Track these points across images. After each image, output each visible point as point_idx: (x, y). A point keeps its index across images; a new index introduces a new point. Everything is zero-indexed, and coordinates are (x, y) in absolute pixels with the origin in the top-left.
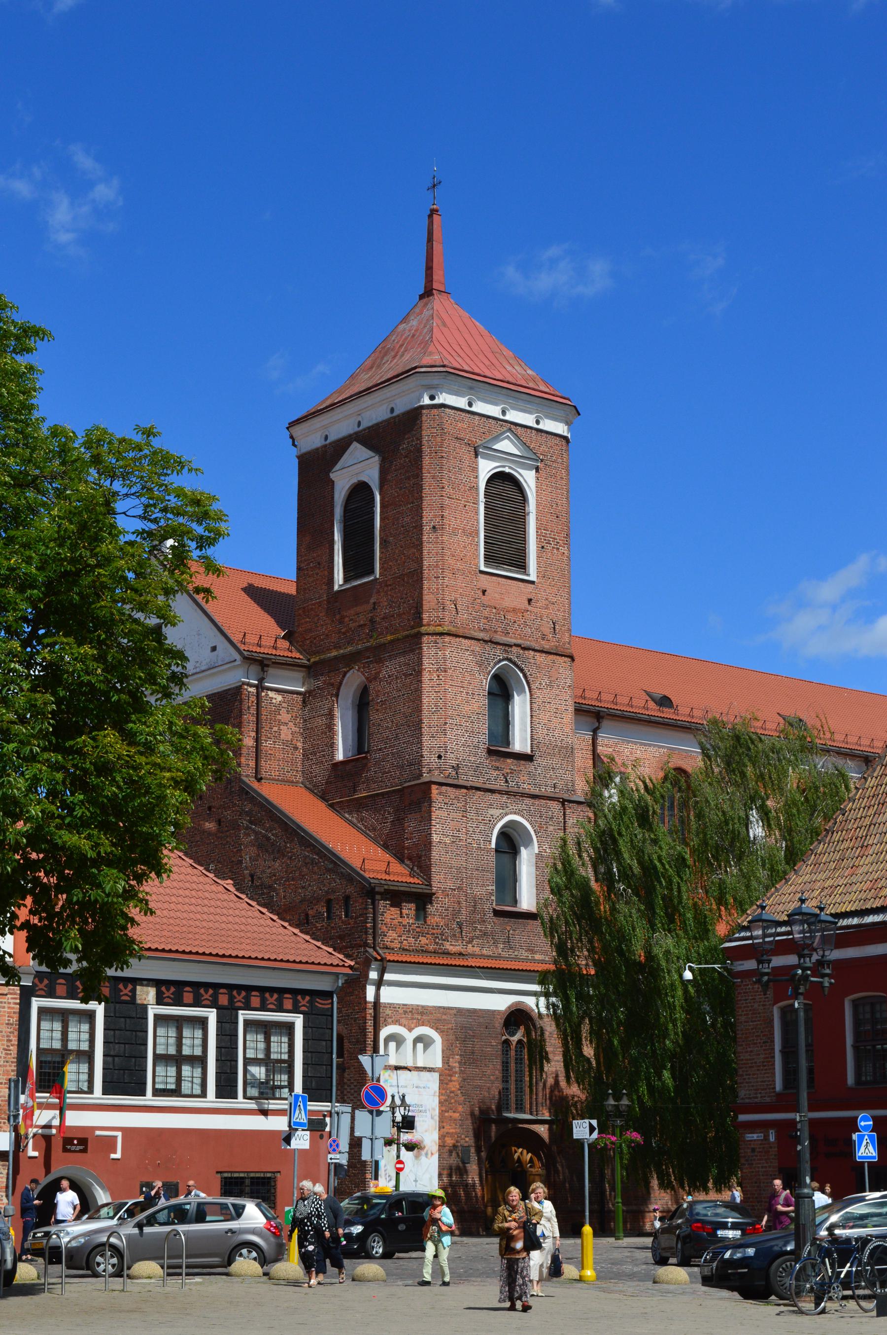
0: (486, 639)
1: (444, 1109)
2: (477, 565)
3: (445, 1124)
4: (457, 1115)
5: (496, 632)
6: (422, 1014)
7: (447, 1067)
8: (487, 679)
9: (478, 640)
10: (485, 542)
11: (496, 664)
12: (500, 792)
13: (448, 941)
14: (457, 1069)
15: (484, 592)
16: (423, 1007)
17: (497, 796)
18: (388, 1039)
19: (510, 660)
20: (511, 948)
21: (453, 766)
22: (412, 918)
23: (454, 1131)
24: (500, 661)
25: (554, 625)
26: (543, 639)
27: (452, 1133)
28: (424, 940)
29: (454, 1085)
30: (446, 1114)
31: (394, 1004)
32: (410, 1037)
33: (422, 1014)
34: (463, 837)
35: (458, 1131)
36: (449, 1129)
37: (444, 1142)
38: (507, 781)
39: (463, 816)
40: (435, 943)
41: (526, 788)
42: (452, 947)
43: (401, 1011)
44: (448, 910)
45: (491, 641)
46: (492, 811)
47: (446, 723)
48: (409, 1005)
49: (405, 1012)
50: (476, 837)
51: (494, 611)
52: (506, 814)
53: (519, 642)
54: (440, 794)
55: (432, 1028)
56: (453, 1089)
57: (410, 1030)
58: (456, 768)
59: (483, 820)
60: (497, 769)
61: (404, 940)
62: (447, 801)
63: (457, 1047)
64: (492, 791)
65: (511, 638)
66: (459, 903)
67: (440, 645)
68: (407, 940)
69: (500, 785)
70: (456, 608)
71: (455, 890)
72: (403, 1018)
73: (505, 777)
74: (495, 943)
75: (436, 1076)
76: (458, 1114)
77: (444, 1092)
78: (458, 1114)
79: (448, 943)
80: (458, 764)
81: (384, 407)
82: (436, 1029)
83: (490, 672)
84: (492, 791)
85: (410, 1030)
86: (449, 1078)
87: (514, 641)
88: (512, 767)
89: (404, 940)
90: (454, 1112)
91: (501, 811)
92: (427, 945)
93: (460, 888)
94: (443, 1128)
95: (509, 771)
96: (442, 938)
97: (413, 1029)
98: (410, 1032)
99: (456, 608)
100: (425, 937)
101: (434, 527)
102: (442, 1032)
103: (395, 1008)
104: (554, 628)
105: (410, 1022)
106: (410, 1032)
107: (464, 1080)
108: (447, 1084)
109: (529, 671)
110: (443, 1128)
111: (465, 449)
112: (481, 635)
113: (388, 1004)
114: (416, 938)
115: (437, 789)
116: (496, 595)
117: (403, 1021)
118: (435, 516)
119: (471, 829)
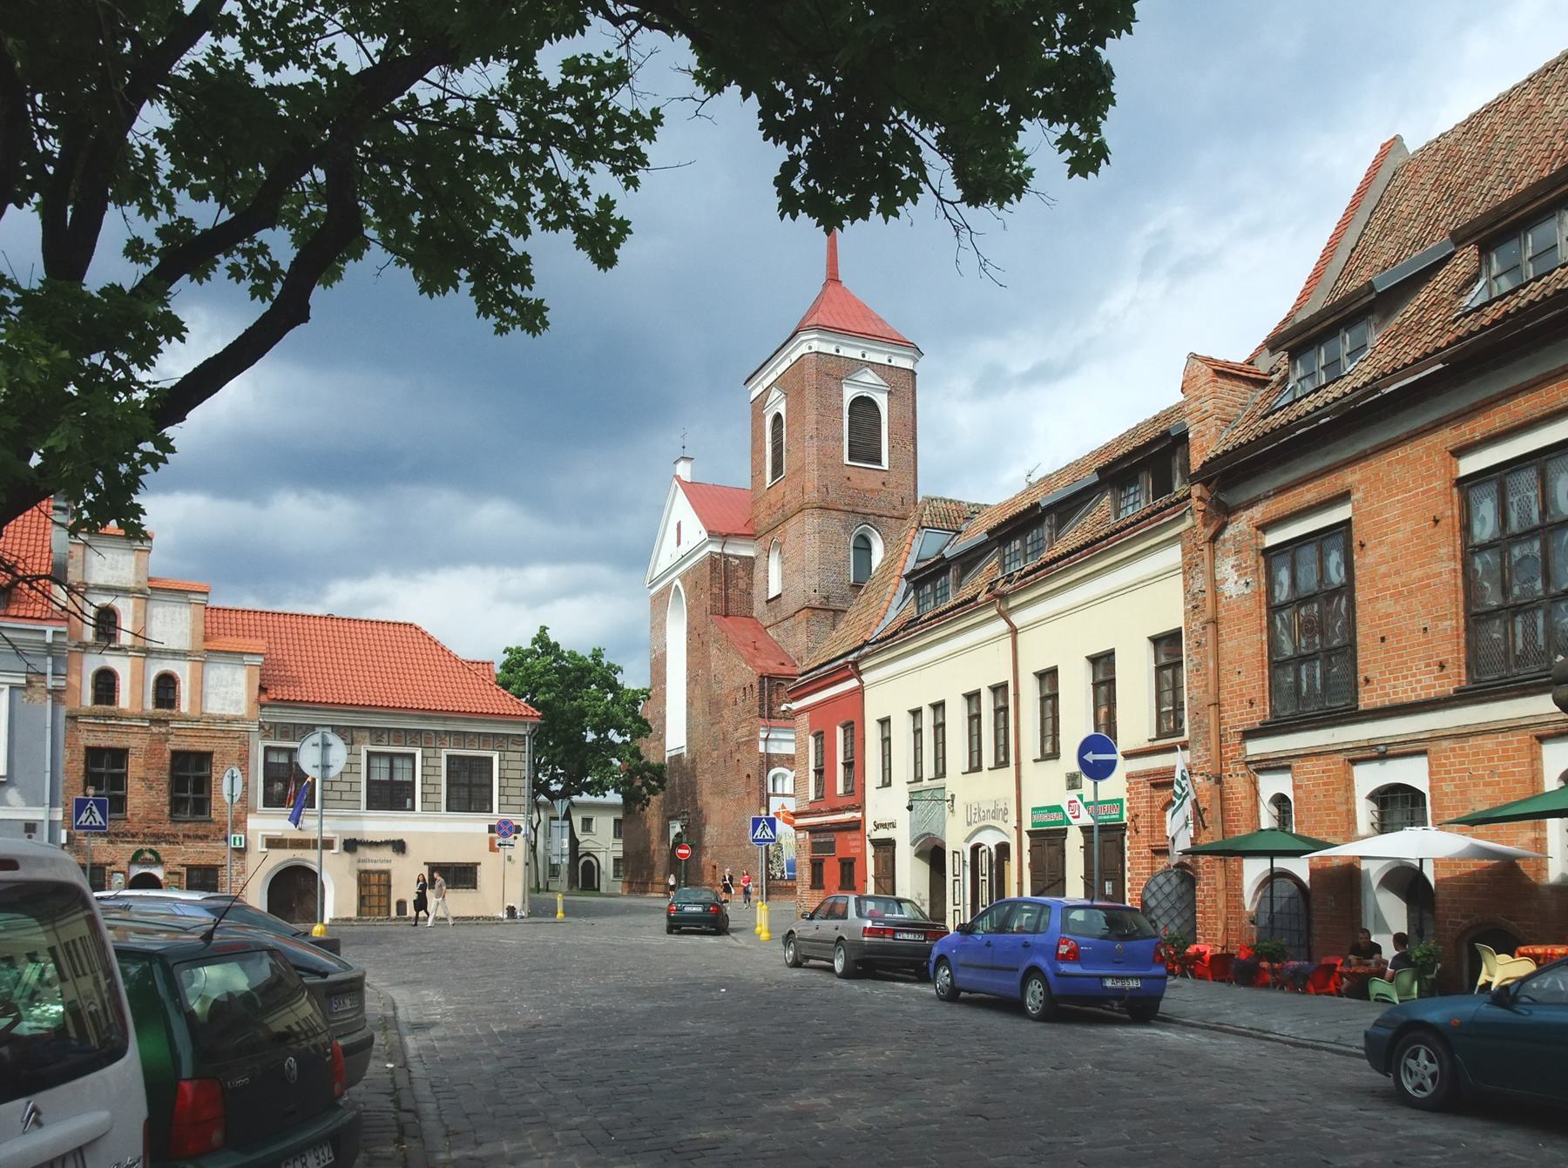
58: (827, 598)
87: (871, 511)
112: (846, 508)
117: (786, 765)
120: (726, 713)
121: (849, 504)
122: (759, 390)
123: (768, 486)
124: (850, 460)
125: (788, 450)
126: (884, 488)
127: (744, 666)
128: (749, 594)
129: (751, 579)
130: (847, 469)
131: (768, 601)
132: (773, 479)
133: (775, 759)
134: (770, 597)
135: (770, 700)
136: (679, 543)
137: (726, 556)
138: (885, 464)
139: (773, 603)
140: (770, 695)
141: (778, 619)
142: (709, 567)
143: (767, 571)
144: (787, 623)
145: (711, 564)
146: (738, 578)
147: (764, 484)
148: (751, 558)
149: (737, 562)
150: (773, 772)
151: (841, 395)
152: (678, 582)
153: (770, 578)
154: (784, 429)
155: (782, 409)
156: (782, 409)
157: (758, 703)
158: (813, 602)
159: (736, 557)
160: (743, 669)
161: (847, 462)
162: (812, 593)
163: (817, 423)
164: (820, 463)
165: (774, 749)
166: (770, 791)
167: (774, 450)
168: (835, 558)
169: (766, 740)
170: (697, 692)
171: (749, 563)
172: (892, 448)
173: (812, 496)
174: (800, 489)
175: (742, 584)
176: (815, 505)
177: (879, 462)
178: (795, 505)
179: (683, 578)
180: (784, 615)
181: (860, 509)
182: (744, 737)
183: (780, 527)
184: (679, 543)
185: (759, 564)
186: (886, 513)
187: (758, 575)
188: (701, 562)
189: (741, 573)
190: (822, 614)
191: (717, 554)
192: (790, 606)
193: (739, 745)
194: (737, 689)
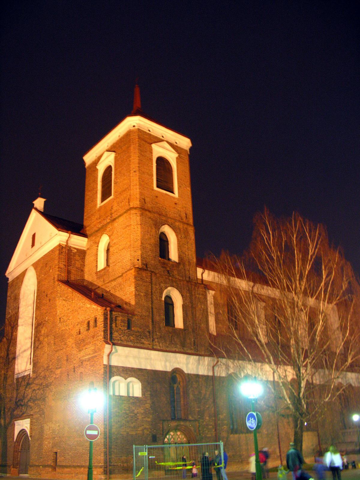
1: (143, 416)
4: (149, 419)
18: (114, 382)
28: (132, 338)
30: (144, 419)
35: (150, 427)
42: (145, 342)
43: (121, 370)
49: (123, 371)
55: (137, 378)
56: (147, 407)
57: (126, 379)
71: (146, 316)
79: (144, 340)
85: (126, 379)
86: (145, 402)
90: (148, 418)
108: (144, 404)
117: (122, 374)
125: (115, 183)
127: (88, 306)
128: (82, 271)
135: (111, 327)
138: (176, 195)
140: (111, 324)
142: (58, 252)
145: (59, 250)
146: (75, 260)
148: (84, 250)
157: (103, 329)
162: (136, 261)
163: (139, 163)
164: (140, 185)
165: (115, 361)
167: (103, 186)
171: (82, 253)
173: (136, 203)
175: (78, 264)
177: (173, 192)
180: (112, 278)
187: (89, 259)
189: (77, 257)
192: (117, 269)
194: (81, 323)
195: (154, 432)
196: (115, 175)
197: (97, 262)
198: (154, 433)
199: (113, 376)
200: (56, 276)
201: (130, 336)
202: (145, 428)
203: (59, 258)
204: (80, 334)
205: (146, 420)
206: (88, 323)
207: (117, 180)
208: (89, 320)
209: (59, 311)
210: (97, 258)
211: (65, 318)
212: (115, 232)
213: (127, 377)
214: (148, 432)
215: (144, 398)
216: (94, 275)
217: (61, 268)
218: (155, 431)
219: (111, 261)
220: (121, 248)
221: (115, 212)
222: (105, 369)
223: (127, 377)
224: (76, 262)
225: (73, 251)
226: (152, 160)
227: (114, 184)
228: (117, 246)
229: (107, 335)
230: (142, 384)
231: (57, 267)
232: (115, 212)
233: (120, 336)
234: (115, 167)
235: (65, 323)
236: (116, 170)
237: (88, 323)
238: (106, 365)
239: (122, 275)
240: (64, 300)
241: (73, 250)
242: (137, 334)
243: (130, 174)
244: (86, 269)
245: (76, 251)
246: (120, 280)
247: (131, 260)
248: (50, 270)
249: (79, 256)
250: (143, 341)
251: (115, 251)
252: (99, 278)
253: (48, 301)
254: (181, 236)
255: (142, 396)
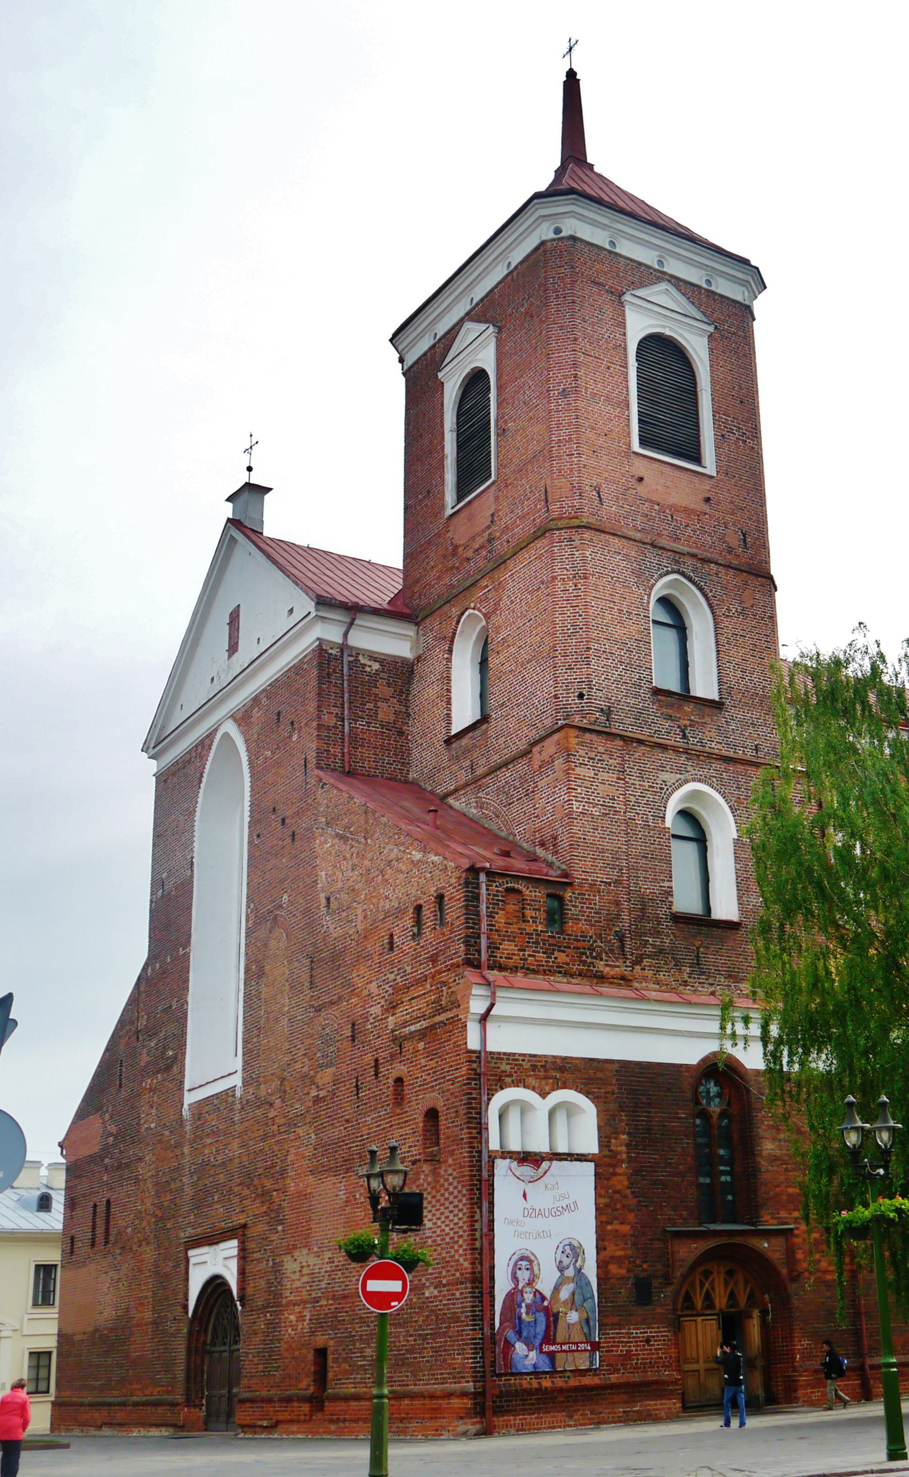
0: (646, 541)
1: (604, 1218)
2: (629, 445)
3: (607, 1243)
4: (626, 1229)
5: (660, 535)
6: (562, 1069)
7: (607, 1153)
8: (649, 595)
9: (635, 540)
10: (639, 419)
11: (661, 576)
12: (675, 749)
13: (601, 960)
14: (624, 1156)
15: (641, 479)
16: (564, 1059)
17: (670, 755)
19: (683, 574)
20: (703, 973)
21: (602, 709)
22: (541, 923)
23: (621, 1253)
24: (668, 573)
25: (744, 535)
26: (729, 552)
27: (620, 1257)
28: (562, 957)
29: (621, 1182)
30: (609, 1227)
31: (514, 1054)
32: (541, 1105)
33: (562, 1069)
34: (620, 807)
35: (629, 1252)
36: (613, 1250)
37: (607, 1272)
38: (684, 736)
39: (618, 778)
40: (581, 961)
41: (715, 747)
43: (527, 1065)
44: (600, 913)
45: (653, 545)
46: (664, 776)
47: (589, 649)
48: (540, 1056)
49: (534, 1068)
50: (641, 810)
51: (656, 507)
52: (687, 781)
53: (695, 551)
54: (581, 744)
55: (580, 1092)
56: (619, 1187)
57: (544, 1095)
58: (607, 713)
59: (650, 786)
60: (669, 717)
61: (529, 955)
62: (592, 755)
63: (621, 1121)
64: (664, 747)
65: (683, 545)
66: (617, 903)
67: (577, 543)
68: (534, 956)
69: (675, 740)
70: (599, 497)
71: (610, 884)
72: (530, 1076)
73: (683, 731)
74: (678, 964)
75: (590, 1167)
76: (628, 1227)
77: (603, 1192)
78: (628, 1227)
79: (602, 963)
80: (609, 707)
81: (500, 267)
82: (587, 1094)
83: (653, 585)
84: (664, 747)
85: (544, 1095)
86: (611, 1170)
87: (686, 549)
88: (692, 718)
89: (529, 955)
90: (622, 1223)
91: (678, 776)
92: (568, 964)
93: (618, 882)
94: (605, 1249)
95: (688, 723)
96: (591, 954)
97: (548, 1093)
98: (544, 1098)
99: (599, 497)
100: (564, 952)
101: (564, 390)
102: (596, 1098)
103: (517, 1060)
104: (745, 540)
105: (543, 1082)
106: (544, 1098)
107: (636, 1172)
108: (608, 1179)
109: (711, 591)
110: (605, 1249)
111: (606, 297)
112: (638, 536)
113: (505, 1054)
114: (549, 953)
115: (577, 737)
116: (659, 487)
117: (532, 1081)
118: (565, 377)
119: (633, 799)
120: (360, 976)
121: (643, 530)
122: (424, 345)
123: (449, 512)
124: (643, 442)
126: (706, 508)
127: (417, 856)
129: (406, 703)
130: (638, 462)
131: (449, 741)
132: (460, 499)
133: (505, 1067)
134: (455, 730)
136: (233, 648)
137: (358, 652)
139: (464, 741)
140: (490, 916)
141: (480, 771)
142: (315, 672)
143: (447, 679)
144: (506, 775)
145: (320, 665)
147: (443, 507)
149: (376, 666)
150: (501, 1098)
151: (623, 325)
152: (230, 728)
153: (454, 695)
154: (493, 395)
155: (487, 359)
156: (487, 359)
157: (463, 933)
158: (577, 718)
159: (373, 656)
160: (415, 864)
161: (636, 446)
162: (573, 699)
166: (494, 1144)
168: (619, 632)
169: (484, 1018)
170: (278, 943)
172: (721, 439)
174: (539, 495)
176: (576, 522)
177: (697, 458)
178: (522, 530)
179: (242, 718)
180: (496, 759)
181: (663, 542)
182: (417, 1019)
183: (484, 583)
184: (233, 648)
185: (430, 671)
186: (716, 557)
188: (297, 670)
189: (383, 689)
190: (601, 745)
191: (333, 644)
193: (399, 1041)
194: (399, 912)
195: (644, 1270)
196: (499, 405)
197: (449, 702)
198: (643, 1275)
199: (502, 1089)
200: (312, 756)
201: (556, 954)
202: (612, 1257)
203: (319, 695)
204: (391, 949)
205: (617, 1231)
206: (418, 909)
207: (506, 422)
208: (421, 902)
209: (323, 873)
210: (449, 691)
211: (344, 897)
212: (505, 601)
213: (547, 1088)
214: (623, 1272)
215: (606, 1156)
216: (440, 746)
217: (328, 728)
218: (645, 1266)
219: (492, 703)
220: (524, 655)
221: (503, 532)
222: (474, 1066)
223: (547, 1088)
224: (379, 704)
225: (368, 669)
226: (625, 349)
227: (498, 435)
228: (512, 649)
229: (479, 952)
230: (598, 1111)
231: (315, 724)
232: (503, 532)
233: (521, 953)
234: (499, 379)
235: (344, 914)
236: (499, 388)
237: (418, 909)
238: (474, 1052)
239: (527, 753)
240: (341, 837)
241: (369, 663)
242: (580, 944)
243: (549, 402)
244: (414, 728)
245: (376, 666)
246: (521, 766)
247: (556, 697)
248: (290, 737)
249: (389, 685)
250: (601, 969)
251: (507, 667)
252: (458, 758)
253: (289, 840)
254: (729, 610)
255: (600, 1151)
